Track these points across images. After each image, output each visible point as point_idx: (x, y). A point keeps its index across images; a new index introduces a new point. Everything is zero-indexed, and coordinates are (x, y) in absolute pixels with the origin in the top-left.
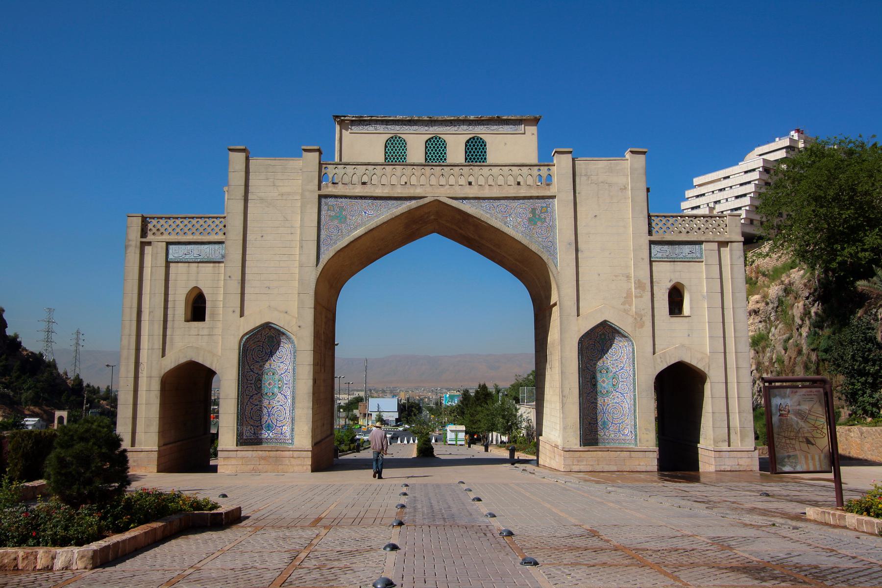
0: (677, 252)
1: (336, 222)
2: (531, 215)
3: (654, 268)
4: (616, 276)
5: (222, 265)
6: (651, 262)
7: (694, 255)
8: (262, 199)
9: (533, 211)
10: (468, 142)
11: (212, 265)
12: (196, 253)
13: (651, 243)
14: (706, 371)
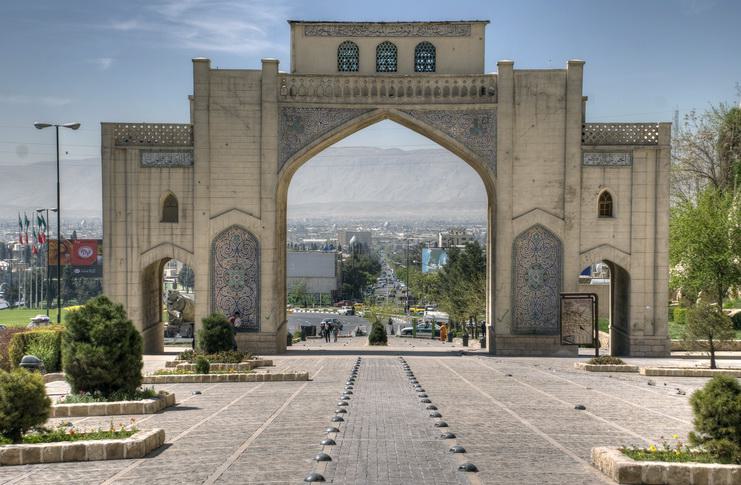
0: (608, 159)
1: (294, 132)
2: (472, 126)
3: (585, 175)
4: (550, 182)
5: (191, 170)
6: (583, 165)
7: (624, 163)
8: (224, 108)
9: (476, 120)
10: (417, 47)
11: (181, 170)
12: (167, 159)
13: (583, 152)
14: (627, 269)
